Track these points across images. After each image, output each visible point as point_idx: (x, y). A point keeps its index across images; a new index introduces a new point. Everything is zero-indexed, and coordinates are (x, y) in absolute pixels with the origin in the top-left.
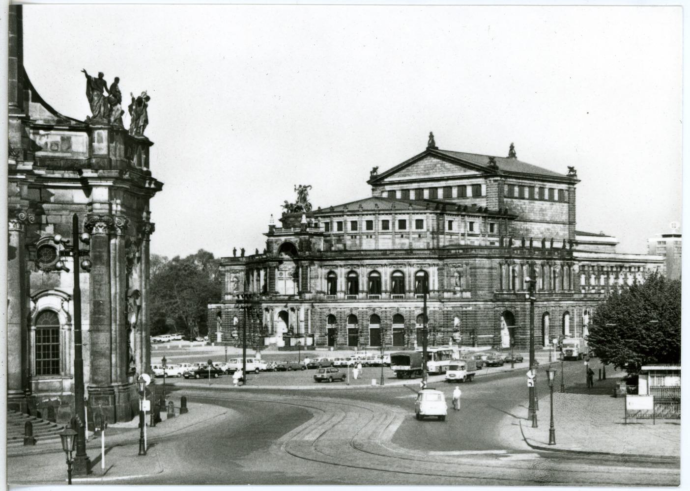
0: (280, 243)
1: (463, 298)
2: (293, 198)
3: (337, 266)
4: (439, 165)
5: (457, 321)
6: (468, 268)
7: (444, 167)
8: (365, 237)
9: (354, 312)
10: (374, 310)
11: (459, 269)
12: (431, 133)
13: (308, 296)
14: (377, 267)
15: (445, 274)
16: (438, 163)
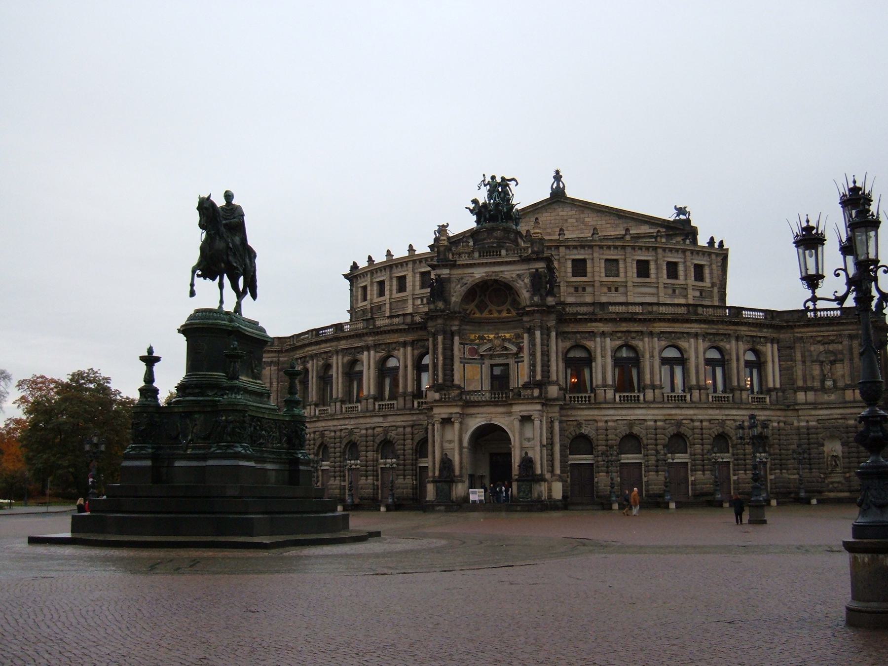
0: (470, 281)
1: (846, 402)
2: (482, 196)
3: (592, 335)
4: (574, 220)
5: (834, 448)
6: (855, 343)
7: (583, 223)
8: (605, 290)
9: (636, 430)
10: (679, 424)
11: (831, 347)
12: (557, 172)
13: (553, 391)
14: (679, 338)
15: (799, 357)
16: (571, 217)
